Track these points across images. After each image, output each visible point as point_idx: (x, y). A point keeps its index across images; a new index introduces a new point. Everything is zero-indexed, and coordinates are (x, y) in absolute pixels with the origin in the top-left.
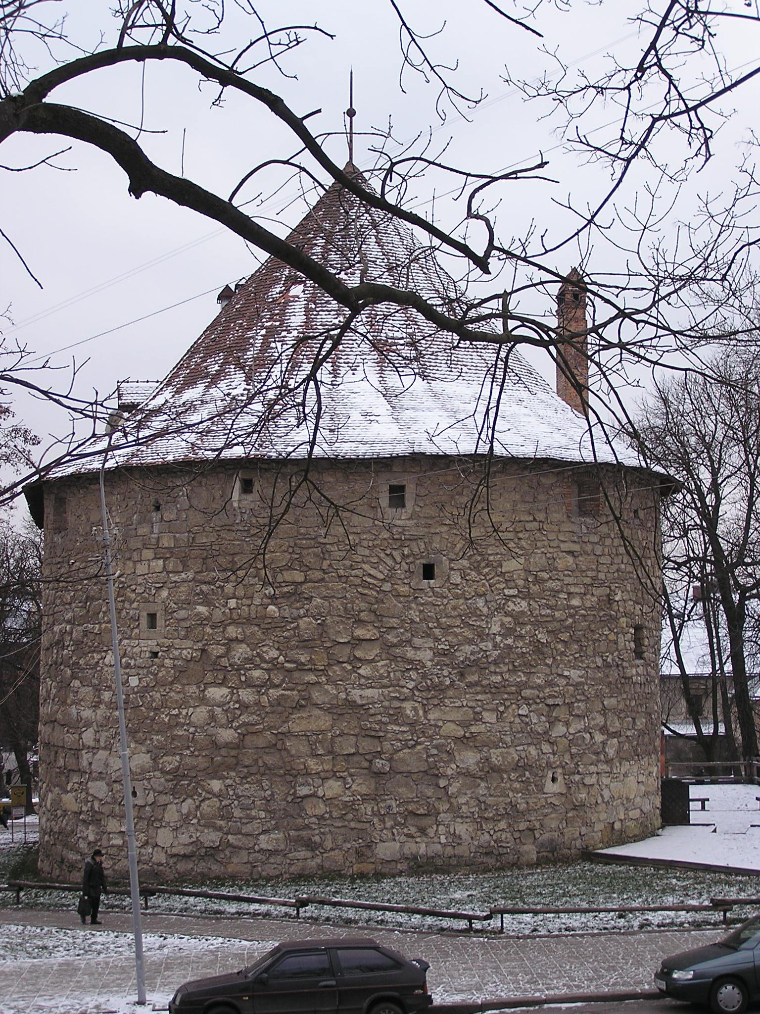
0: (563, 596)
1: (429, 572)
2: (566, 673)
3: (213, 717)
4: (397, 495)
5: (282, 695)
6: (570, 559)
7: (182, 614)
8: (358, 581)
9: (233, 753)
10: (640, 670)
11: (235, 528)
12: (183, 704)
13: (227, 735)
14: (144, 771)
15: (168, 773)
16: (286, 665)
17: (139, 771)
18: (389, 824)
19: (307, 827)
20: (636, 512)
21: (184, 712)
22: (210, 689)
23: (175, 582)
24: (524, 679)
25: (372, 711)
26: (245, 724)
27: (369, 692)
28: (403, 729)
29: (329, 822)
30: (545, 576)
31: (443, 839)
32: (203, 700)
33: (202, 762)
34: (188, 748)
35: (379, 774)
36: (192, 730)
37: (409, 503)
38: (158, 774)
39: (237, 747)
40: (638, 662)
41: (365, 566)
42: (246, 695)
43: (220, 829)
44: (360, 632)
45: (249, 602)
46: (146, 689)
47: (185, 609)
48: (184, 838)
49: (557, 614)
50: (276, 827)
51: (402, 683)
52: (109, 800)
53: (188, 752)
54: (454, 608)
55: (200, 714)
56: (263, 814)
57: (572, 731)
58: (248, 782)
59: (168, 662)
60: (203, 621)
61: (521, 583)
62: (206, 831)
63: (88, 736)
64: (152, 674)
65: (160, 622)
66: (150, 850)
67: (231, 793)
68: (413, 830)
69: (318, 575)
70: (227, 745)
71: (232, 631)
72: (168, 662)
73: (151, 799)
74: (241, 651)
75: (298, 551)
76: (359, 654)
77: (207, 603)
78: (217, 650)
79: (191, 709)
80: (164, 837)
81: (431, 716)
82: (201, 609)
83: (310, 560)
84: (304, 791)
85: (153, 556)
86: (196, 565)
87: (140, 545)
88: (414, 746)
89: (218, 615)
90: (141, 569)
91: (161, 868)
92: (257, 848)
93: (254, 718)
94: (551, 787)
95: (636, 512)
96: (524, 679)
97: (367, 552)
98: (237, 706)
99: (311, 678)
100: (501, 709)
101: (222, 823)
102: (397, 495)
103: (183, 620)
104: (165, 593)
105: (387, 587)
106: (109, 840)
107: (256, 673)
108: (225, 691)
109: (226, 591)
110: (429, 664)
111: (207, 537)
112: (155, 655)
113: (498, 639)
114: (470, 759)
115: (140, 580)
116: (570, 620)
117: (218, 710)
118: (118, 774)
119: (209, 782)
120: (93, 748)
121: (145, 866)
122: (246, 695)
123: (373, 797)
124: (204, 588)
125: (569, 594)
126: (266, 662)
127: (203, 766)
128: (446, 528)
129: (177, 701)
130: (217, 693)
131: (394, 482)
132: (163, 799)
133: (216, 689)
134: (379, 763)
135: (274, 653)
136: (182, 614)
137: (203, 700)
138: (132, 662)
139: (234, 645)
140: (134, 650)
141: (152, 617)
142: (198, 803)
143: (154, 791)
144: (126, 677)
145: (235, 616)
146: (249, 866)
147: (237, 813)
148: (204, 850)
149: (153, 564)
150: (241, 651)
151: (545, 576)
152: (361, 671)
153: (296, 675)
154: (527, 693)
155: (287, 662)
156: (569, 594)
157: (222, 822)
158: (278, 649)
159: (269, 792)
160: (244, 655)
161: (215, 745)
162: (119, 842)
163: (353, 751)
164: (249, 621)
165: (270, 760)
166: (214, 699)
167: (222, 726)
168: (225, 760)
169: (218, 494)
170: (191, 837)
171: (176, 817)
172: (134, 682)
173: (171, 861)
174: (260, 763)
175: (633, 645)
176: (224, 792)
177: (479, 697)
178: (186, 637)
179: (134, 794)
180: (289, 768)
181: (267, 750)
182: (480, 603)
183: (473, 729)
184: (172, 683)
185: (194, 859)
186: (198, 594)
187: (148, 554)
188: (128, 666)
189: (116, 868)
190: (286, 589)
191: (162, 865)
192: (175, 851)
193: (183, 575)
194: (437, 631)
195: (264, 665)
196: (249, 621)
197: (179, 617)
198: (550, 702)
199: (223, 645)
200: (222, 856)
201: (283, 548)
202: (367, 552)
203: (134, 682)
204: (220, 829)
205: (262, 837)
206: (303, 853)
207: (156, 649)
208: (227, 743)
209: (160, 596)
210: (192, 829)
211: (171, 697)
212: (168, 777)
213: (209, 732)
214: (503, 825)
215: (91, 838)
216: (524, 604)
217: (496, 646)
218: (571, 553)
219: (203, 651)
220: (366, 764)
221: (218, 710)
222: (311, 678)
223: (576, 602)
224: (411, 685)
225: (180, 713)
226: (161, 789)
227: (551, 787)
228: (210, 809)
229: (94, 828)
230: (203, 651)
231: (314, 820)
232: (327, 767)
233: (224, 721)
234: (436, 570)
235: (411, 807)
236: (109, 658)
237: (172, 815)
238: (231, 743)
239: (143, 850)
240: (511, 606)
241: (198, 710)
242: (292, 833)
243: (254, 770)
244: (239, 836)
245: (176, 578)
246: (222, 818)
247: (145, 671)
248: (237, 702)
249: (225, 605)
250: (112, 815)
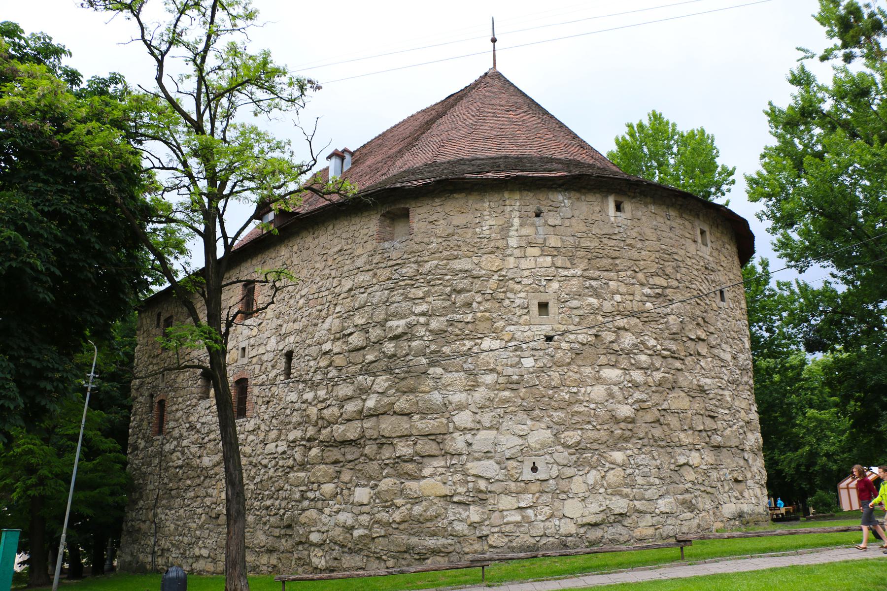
3: (611, 395)
5: (664, 377)
7: (575, 303)
8: (695, 293)
9: (630, 426)
11: (614, 237)
12: (580, 383)
13: (625, 411)
14: (544, 446)
15: (569, 447)
16: (665, 353)
17: (538, 446)
18: (727, 488)
19: (687, 491)
21: (583, 390)
22: (605, 370)
23: (565, 276)
25: (711, 396)
26: (636, 402)
27: (708, 381)
28: (727, 411)
29: (697, 487)
32: (598, 380)
33: (603, 435)
34: (589, 423)
36: (593, 406)
37: (709, 244)
38: (560, 448)
39: (633, 421)
42: (638, 376)
43: (627, 496)
45: (631, 298)
46: (542, 369)
47: (576, 299)
48: (594, 507)
50: (668, 493)
51: (722, 375)
52: (501, 477)
53: (590, 427)
55: (598, 392)
56: (657, 481)
58: (643, 453)
59: (564, 345)
60: (595, 311)
62: (614, 498)
63: (463, 419)
64: (548, 355)
65: (553, 308)
66: (557, 523)
67: (632, 462)
68: (737, 494)
69: (675, 283)
70: (625, 420)
71: (621, 322)
72: (564, 345)
73: (555, 472)
74: (628, 340)
75: (662, 262)
77: (597, 296)
78: (609, 337)
79: (589, 389)
80: (573, 508)
82: (592, 300)
83: (669, 270)
84: (682, 460)
85: (539, 253)
86: (583, 265)
87: (524, 244)
89: (607, 306)
90: (524, 264)
91: (570, 539)
92: (657, 511)
93: (644, 396)
97: (696, 273)
98: (630, 385)
101: (628, 490)
103: (575, 308)
104: (555, 285)
106: (503, 517)
107: (643, 358)
109: (611, 287)
110: (731, 364)
111: (591, 242)
112: (549, 339)
115: (526, 273)
117: (615, 389)
118: (514, 451)
119: (610, 453)
120: (472, 429)
121: (551, 539)
122: (638, 376)
123: (715, 467)
124: (594, 283)
126: (648, 349)
127: (604, 439)
128: (722, 269)
129: (575, 380)
132: (568, 472)
133: (610, 370)
135: (652, 342)
136: (575, 303)
137: (598, 380)
138: (524, 346)
139: (622, 332)
140: (525, 334)
142: (603, 473)
143: (558, 464)
144: (517, 359)
145: (622, 310)
146: (653, 528)
147: (640, 480)
148: (613, 517)
149: (541, 259)
153: (670, 360)
155: (663, 349)
157: (627, 490)
158: (656, 339)
159: (659, 461)
160: (631, 342)
161: (616, 420)
162: (517, 517)
163: (702, 428)
164: (632, 314)
165: (657, 432)
166: (610, 379)
167: (619, 403)
168: (623, 432)
169: (598, 209)
170: (601, 505)
171: (584, 488)
172: (528, 363)
173: (582, 530)
174: (650, 436)
176: (627, 461)
178: (579, 324)
179: (534, 469)
180: (669, 440)
181: (653, 425)
184: (569, 364)
185: (603, 526)
186: (587, 288)
187: (531, 251)
189: (514, 544)
190: (657, 291)
191: (571, 536)
192: (586, 520)
193: (572, 272)
195: (649, 352)
196: (632, 314)
197: (573, 306)
199: (614, 332)
200: (630, 521)
201: (652, 258)
202: (696, 273)
203: (528, 363)
204: (627, 496)
205: (660, 501)
206: (688, 515)
207: (551, 333)
208: (626, 418)
209: (550, 287)
210: (601, 498)
211: (570, 377)
212: (572, 450)
213: (609, 408)
215: (475, 518)
221: (615, 389)
222: (678, 364)
225: (579, 391)
226: (565, 462)
228: (615, 478)
229: (477, 508)
230: (596, 336)
231: (690, 485)
232: (691, 441)
233: (621, 398)
235: (735, 474)
237: (578, 486)
238: (629, 417)
239: (547, 523)
241: (596, 388)
242: (680, 497)
243: (646, 441)
244: (644, 502)
245: (565, 273)
246: (627, 485)
247: (541, 353)
248: (629, 382)
250: (507, 492)
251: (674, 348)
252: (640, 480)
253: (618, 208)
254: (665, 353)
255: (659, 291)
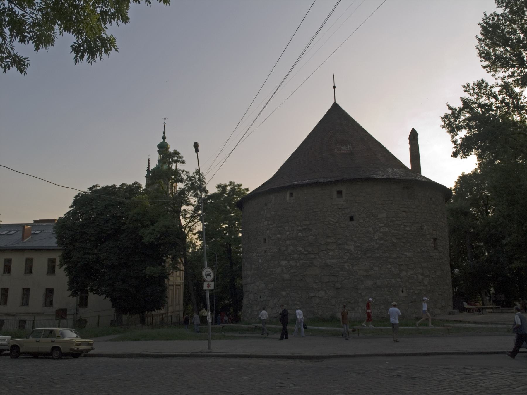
0: (402, 226)
1: (352, 219)
2: (405, 254)
4: (340, 193)
6: (404, 214)
10: (437, 254)
13: (287, 276)
16: (305, 252)
20: (431, 199)
24: (388, 255)
27: (333, 261)
30: (394, 219)
31: (360, 311)
35: (337, 288)
40: (436, 251)
41: (330, 218)
42: (292, 263)
44: (329, 240)
49: (400, 233)
54: (361, 231)
55: (279, 270)
56: (299, 303)
57: (409, 274)
61: (385, 222)
65: (267, 241)
71: (288, 242)
74: (291, 248)
76: (329, 248)
81: (354, 268)
82: (279, 236)
84: (312, 295)
88: (348, 279)
94: (401, 294)
95: (431, 199)
96: (388, 255)
97: (330, 213)
99: (313, 256)
100: (380, 266)
102: (340, 193)
104: (268, 232)
105: (337, 225)
107: (295, 256)
108: (286, 262)
112: (266, 251)
113: (378, 241)
114: (369, 283)
116: (406, 235)
117: (284, 268)
122: (292, 263)
124: (279, 229)
125: (405, 226)
128: (357, 204)
130: (284, 263)
131: (338, 190)
134: (337, 285)
135: (301, 249)
141: (265, 239)
147: (290, 303)
150: (291, 248)
151: (394, 219)
152: (330, 254)
154: (390, 260)
156: (405, 226)
172: (260, 261)
175: (433, 245)
177: (372, 261)
182: (371, 229)
183: (370, 273)
188: (258, 256)
194: (355, 239)
198: (400, 263)
202: (330, 213)
214: (382, 307)
216: (387, 229)
217: (377, 244)
218: (404, 211)
219: (279, 249)
220: (332, 285)
221: (284, 268)
222: (313, 256)
223: (408, 229)
224: (347, 258)
227: (401, 294)
234: (354, 218)
236: (255, 254)
240: (382, 230)
245: (271, 226)
249: (286, 234)
251: (310, 250)
252: (290, 303)
253: (291, 195)
254: (305, 252)
255: (305, 227)
